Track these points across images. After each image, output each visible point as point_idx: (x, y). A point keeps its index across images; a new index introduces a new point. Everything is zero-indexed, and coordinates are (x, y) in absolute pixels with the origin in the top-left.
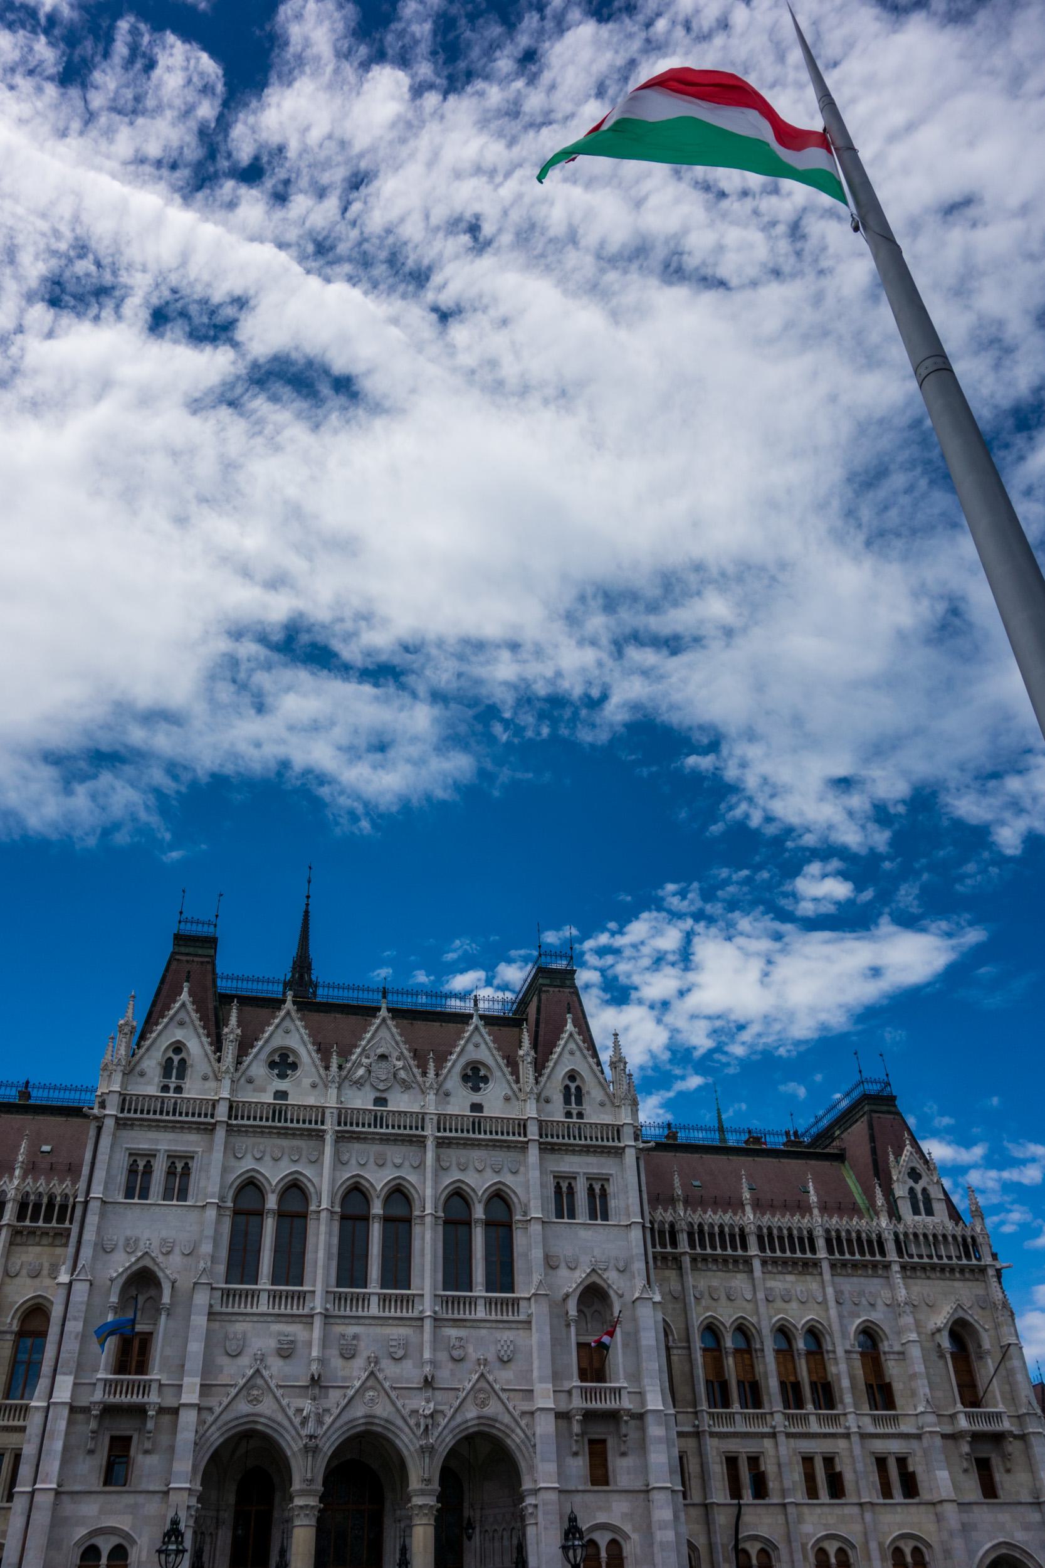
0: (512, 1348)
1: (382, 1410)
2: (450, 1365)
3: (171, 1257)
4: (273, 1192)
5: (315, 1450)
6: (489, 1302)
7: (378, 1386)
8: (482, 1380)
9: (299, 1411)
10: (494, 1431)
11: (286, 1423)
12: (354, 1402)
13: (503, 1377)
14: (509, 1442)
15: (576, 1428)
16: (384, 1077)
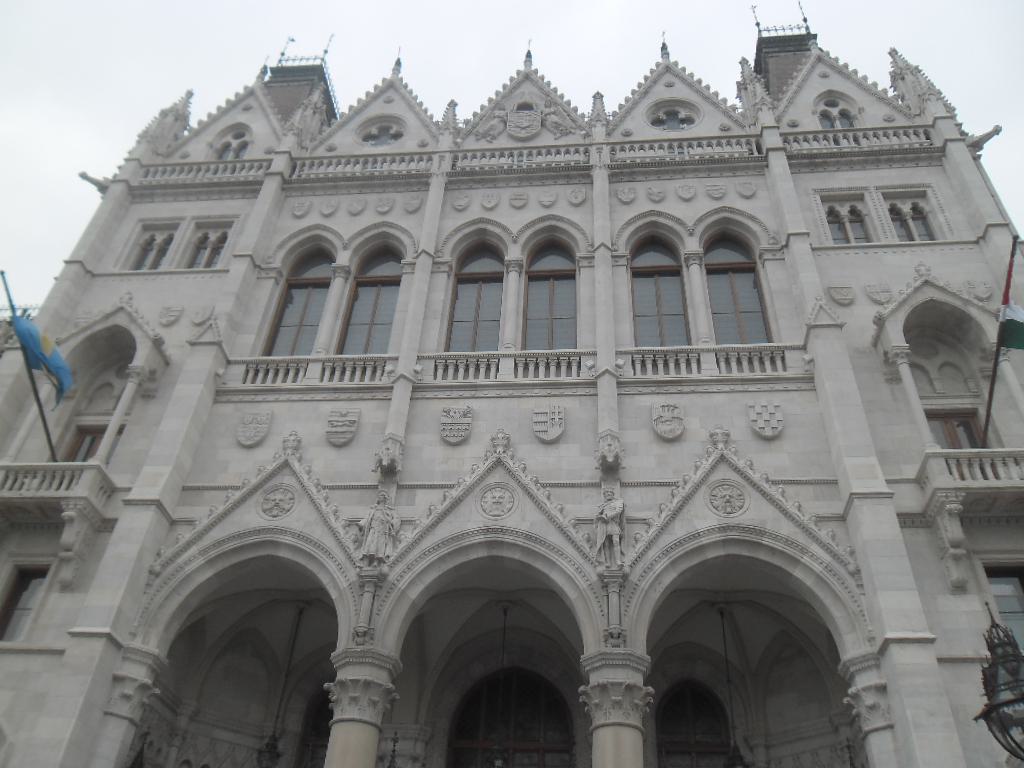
0: (779, 416)
1: (522, 519)
2: (658, 449)
3: (175, 328)
4: (345, 248)
5: (379, 581)
6: (724, 358)
7: (513, 483)
9: (352, 523)
10: (762, 556)
11: (329, 542)
12: (463, 508)
13: (768, 463)
14: (798, 573)
15: (953, 530)
16: (526, 124)
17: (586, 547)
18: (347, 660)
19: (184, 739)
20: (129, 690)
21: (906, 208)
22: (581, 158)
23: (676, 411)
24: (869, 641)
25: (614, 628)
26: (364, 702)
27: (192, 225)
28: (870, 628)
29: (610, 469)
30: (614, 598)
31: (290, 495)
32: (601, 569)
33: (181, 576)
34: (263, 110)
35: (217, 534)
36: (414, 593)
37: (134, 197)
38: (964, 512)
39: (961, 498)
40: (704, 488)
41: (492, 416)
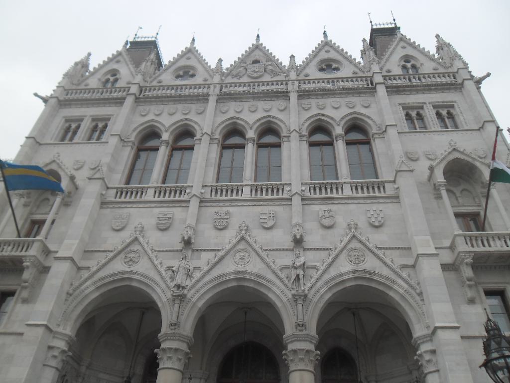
1: (254, 267)
2: (321, 232)
4: (166, 131)
5: (182, 298)
6: (355, 187)
8: (354, 241)
9: (169, 268)
10: (373, 285)
11: (157, 278)
12: (225, 261)
14: (391, 294)
15: (468, 272)
17: (286, 281)
18: (166, 338)
19: (84, 378)
20: (56, 353)
21: (444, 112)
22: (283, 87)
23: (331, 212)
24: (427, 328)
25: (300, 321)
26: (175, 359)
27: (90, 120)
28: (427, 321)
29: (298, 242)
30: (300, 306)
31: (138, 255)
32: (294, 292)
33: (83, 295)
34: (126, 62)
35: (102, 274)
36: (200, 304)
37: (61, 105)
38: (474, 263)
39: (472, 257)
40: (345, 251)
41: (240, 215)
